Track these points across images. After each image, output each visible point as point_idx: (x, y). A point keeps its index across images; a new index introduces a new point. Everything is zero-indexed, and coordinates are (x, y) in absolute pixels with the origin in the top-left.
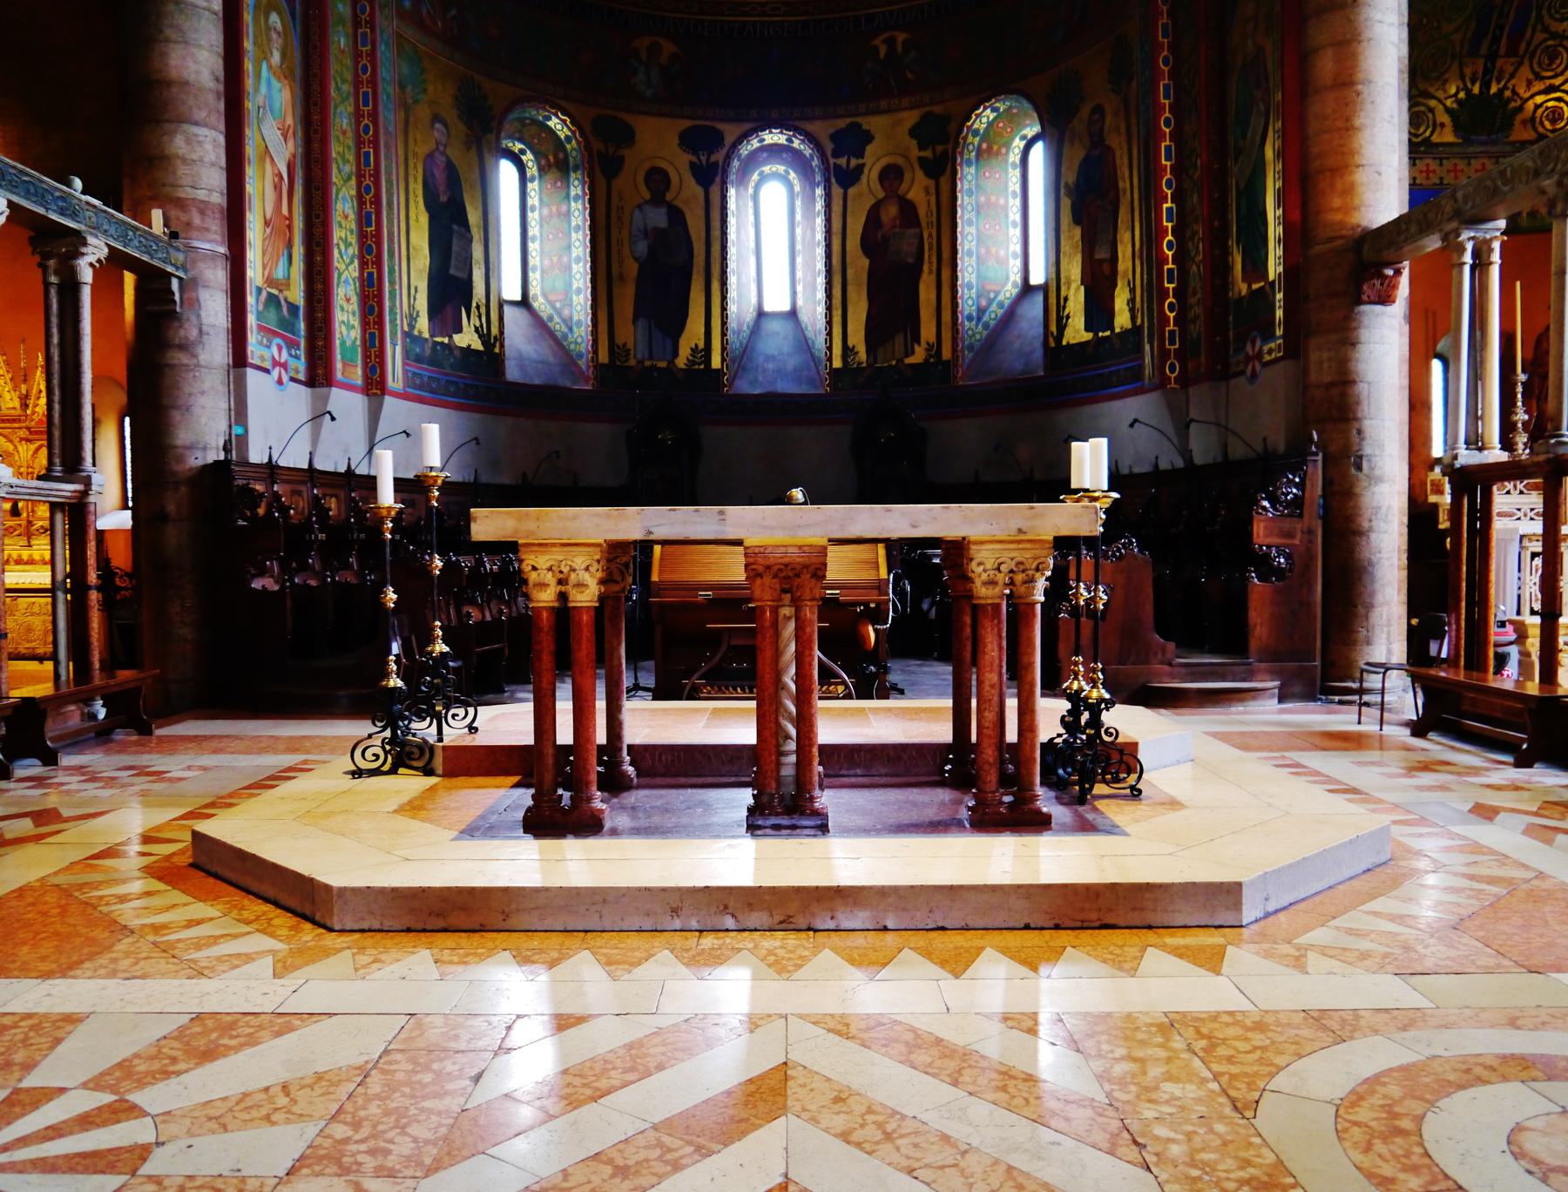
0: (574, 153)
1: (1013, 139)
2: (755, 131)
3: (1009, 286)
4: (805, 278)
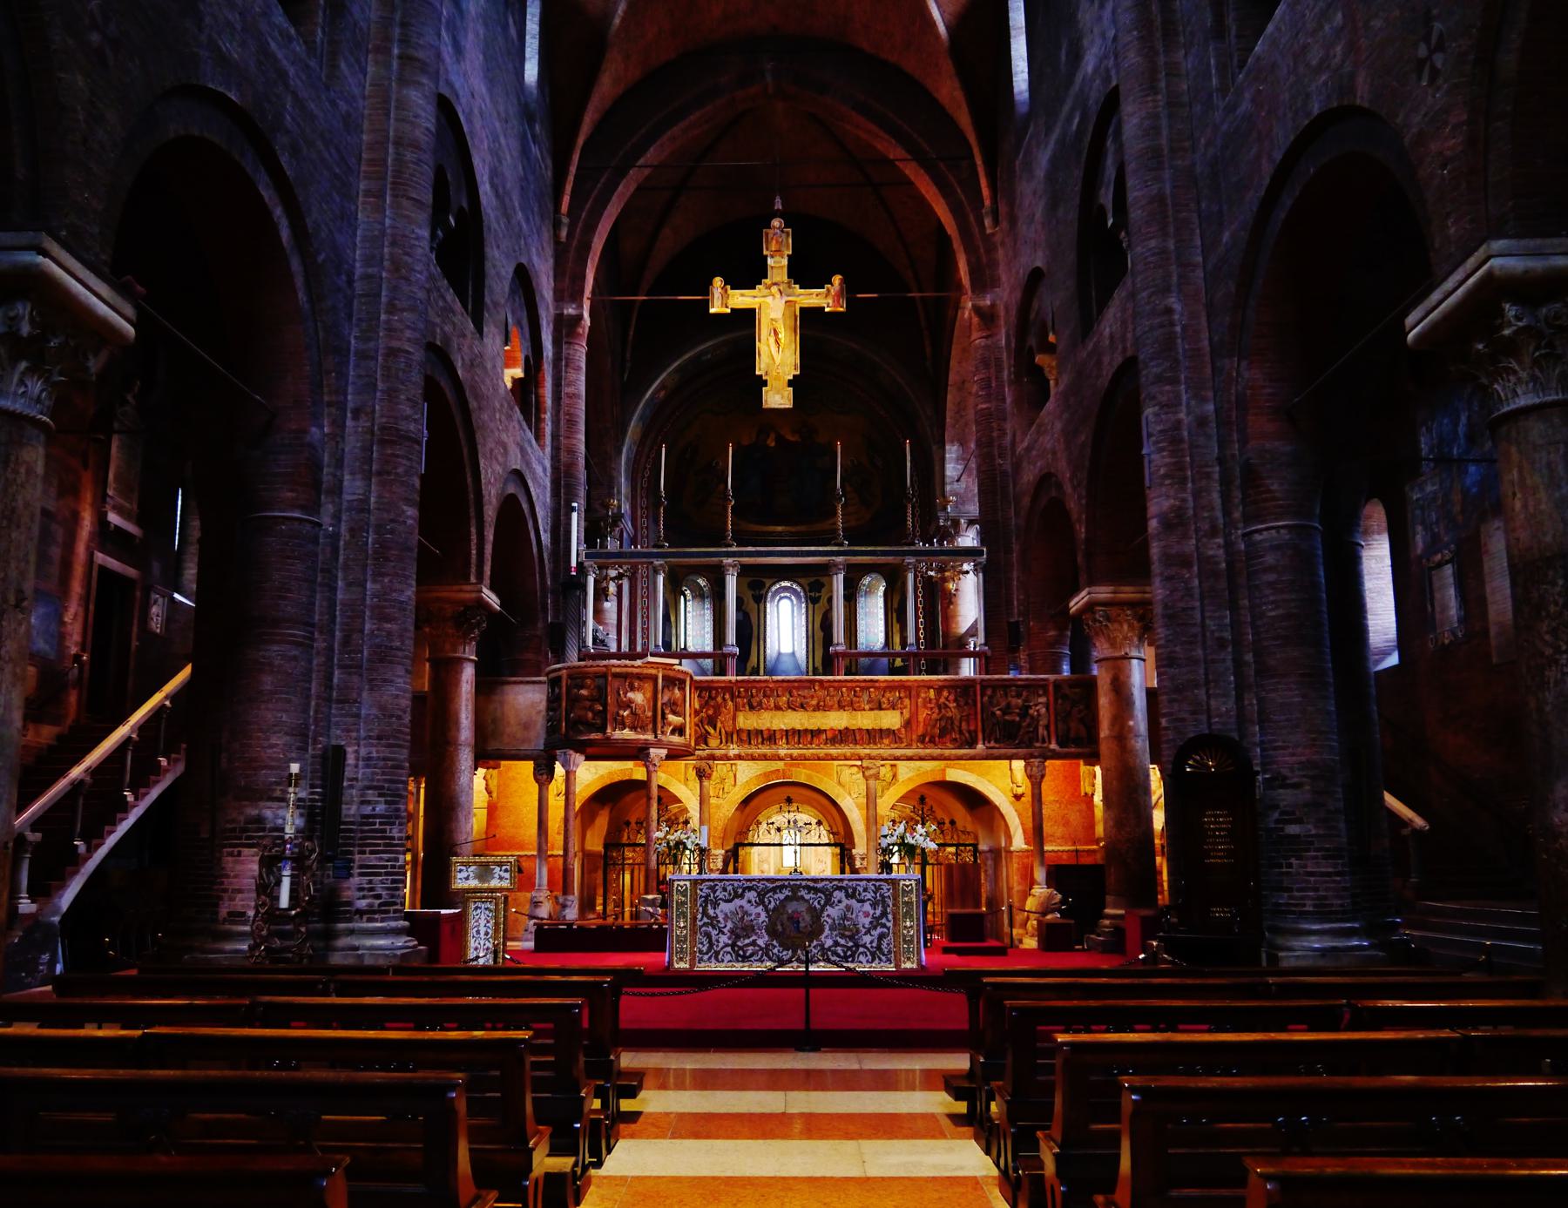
2: (778, 582)
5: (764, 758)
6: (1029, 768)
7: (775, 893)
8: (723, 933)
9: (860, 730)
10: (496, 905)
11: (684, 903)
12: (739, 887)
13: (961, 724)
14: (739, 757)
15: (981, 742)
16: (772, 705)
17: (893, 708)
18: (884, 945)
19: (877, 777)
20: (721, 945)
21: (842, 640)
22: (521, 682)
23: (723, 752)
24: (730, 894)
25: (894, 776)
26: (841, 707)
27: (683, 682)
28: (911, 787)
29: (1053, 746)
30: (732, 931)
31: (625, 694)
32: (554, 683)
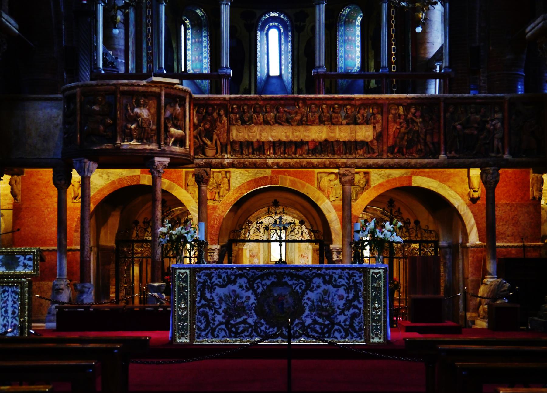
0: (204, 21)
1: (357, 17)
2: (268, 12)
3: (356, 68)
4: (285, 64)
5: (254, 166)
6: (484, 175)
7: (263, 279)
8: (219, 313)
9: (338, 141)
10: (22, 288)
11: (184, 288)
12: (232, 274)
13: (426, 136)
14: (232, 165)
15: (443, 153)
16: (262, 120)
17: (367, 122)
18: (356, 324)
19: (351, 182)
20: (217, 323)
21: (323, 63)
22: (40, 99)
23: (218, 160)
24: (224, 281)
25: (367, 182)
26: (321, 122)
27: (183, 99)
28: (381, 192)
29: (506, 156)
30: (225, 311)
31: (132, 110)
32: (69, 99)
